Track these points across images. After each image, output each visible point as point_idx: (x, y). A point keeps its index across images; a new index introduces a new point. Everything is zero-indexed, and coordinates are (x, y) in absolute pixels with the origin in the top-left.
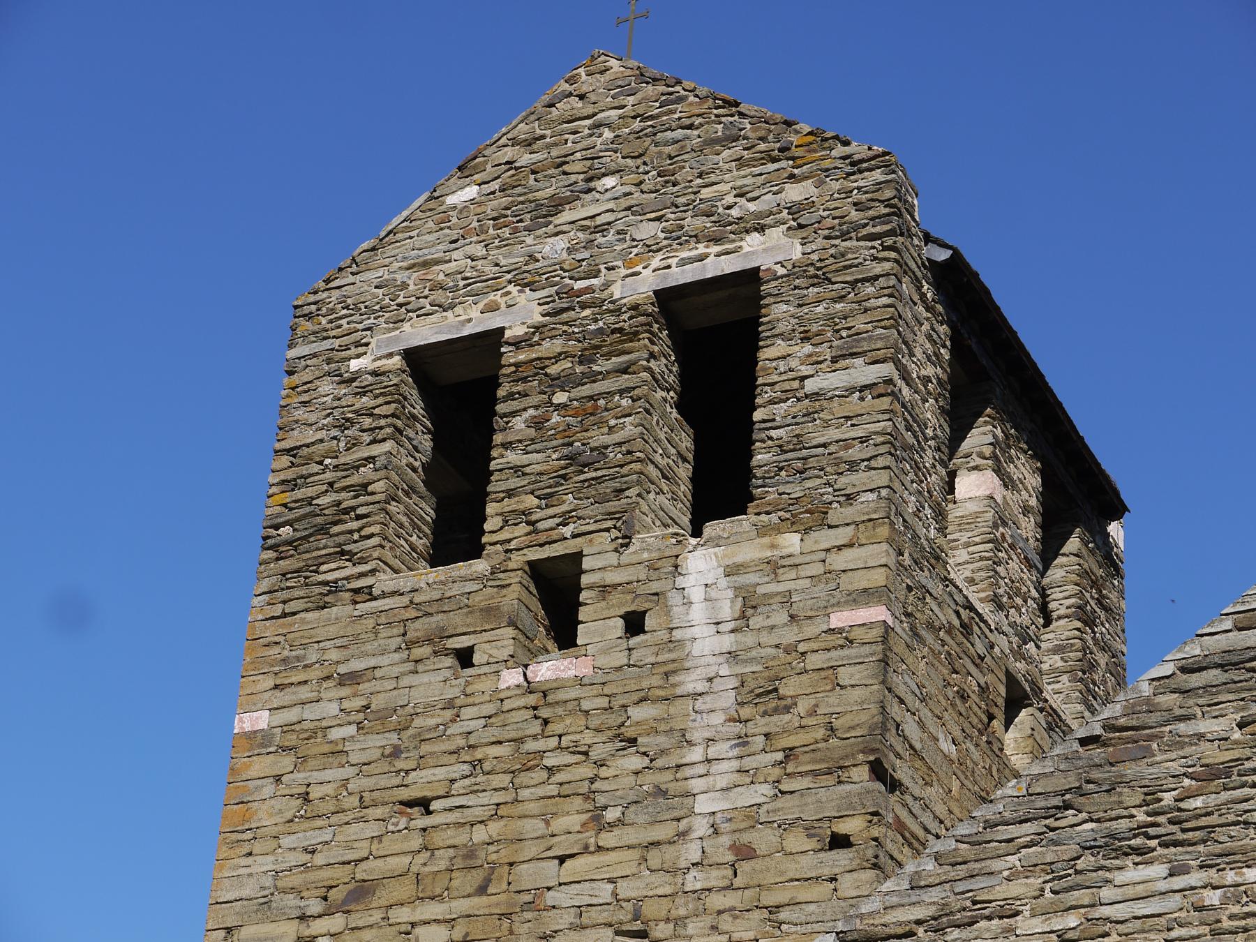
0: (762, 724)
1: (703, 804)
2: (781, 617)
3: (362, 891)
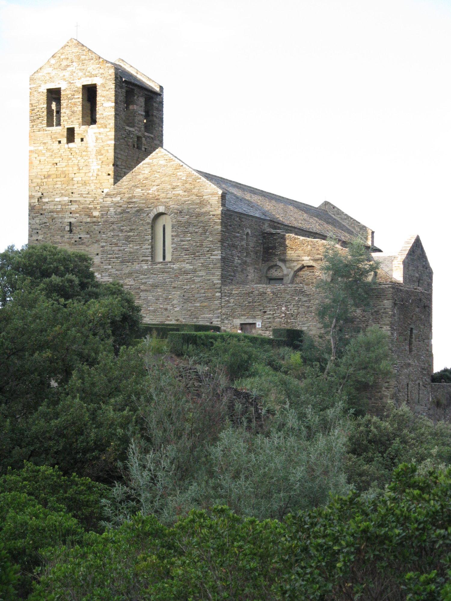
0: (99, 157)
1: (92, 168)
2: (101, 141)
3: (49, 176)
